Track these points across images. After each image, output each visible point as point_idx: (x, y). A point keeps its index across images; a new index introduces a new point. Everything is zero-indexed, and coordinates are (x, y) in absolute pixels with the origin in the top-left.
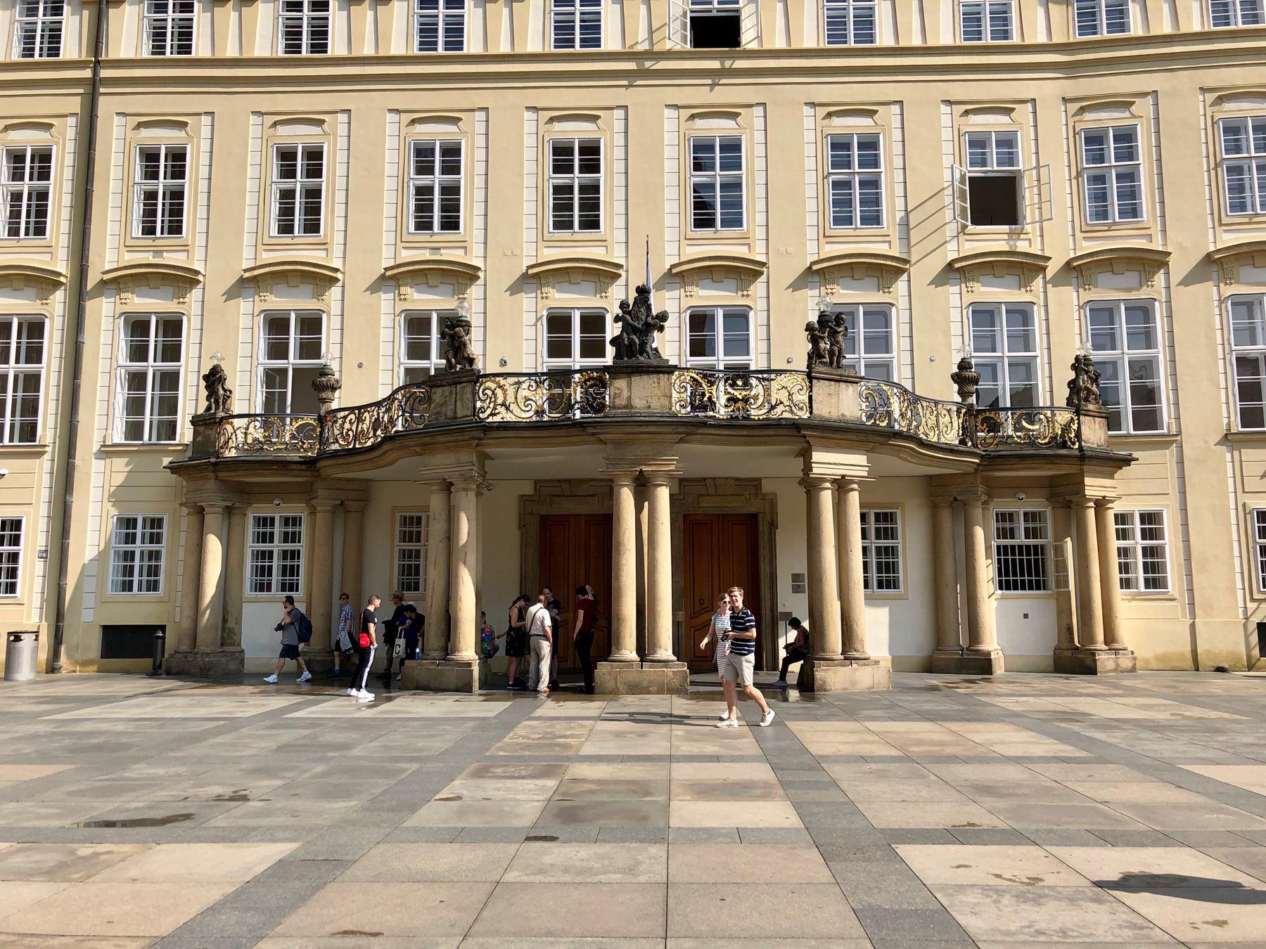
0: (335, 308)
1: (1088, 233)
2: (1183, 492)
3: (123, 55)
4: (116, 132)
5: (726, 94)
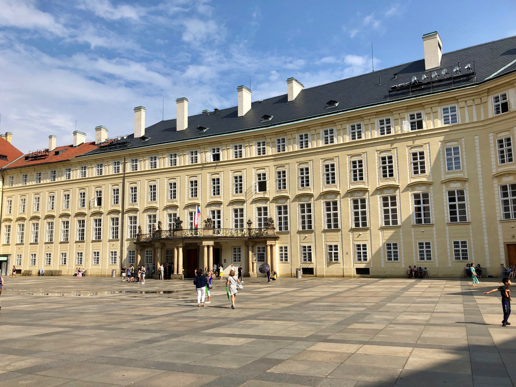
0: (158, 214)
1: (277, 192)
2: (291, 243)
3: (128, 172)
4: (127, 185)
5: (217, 170)
